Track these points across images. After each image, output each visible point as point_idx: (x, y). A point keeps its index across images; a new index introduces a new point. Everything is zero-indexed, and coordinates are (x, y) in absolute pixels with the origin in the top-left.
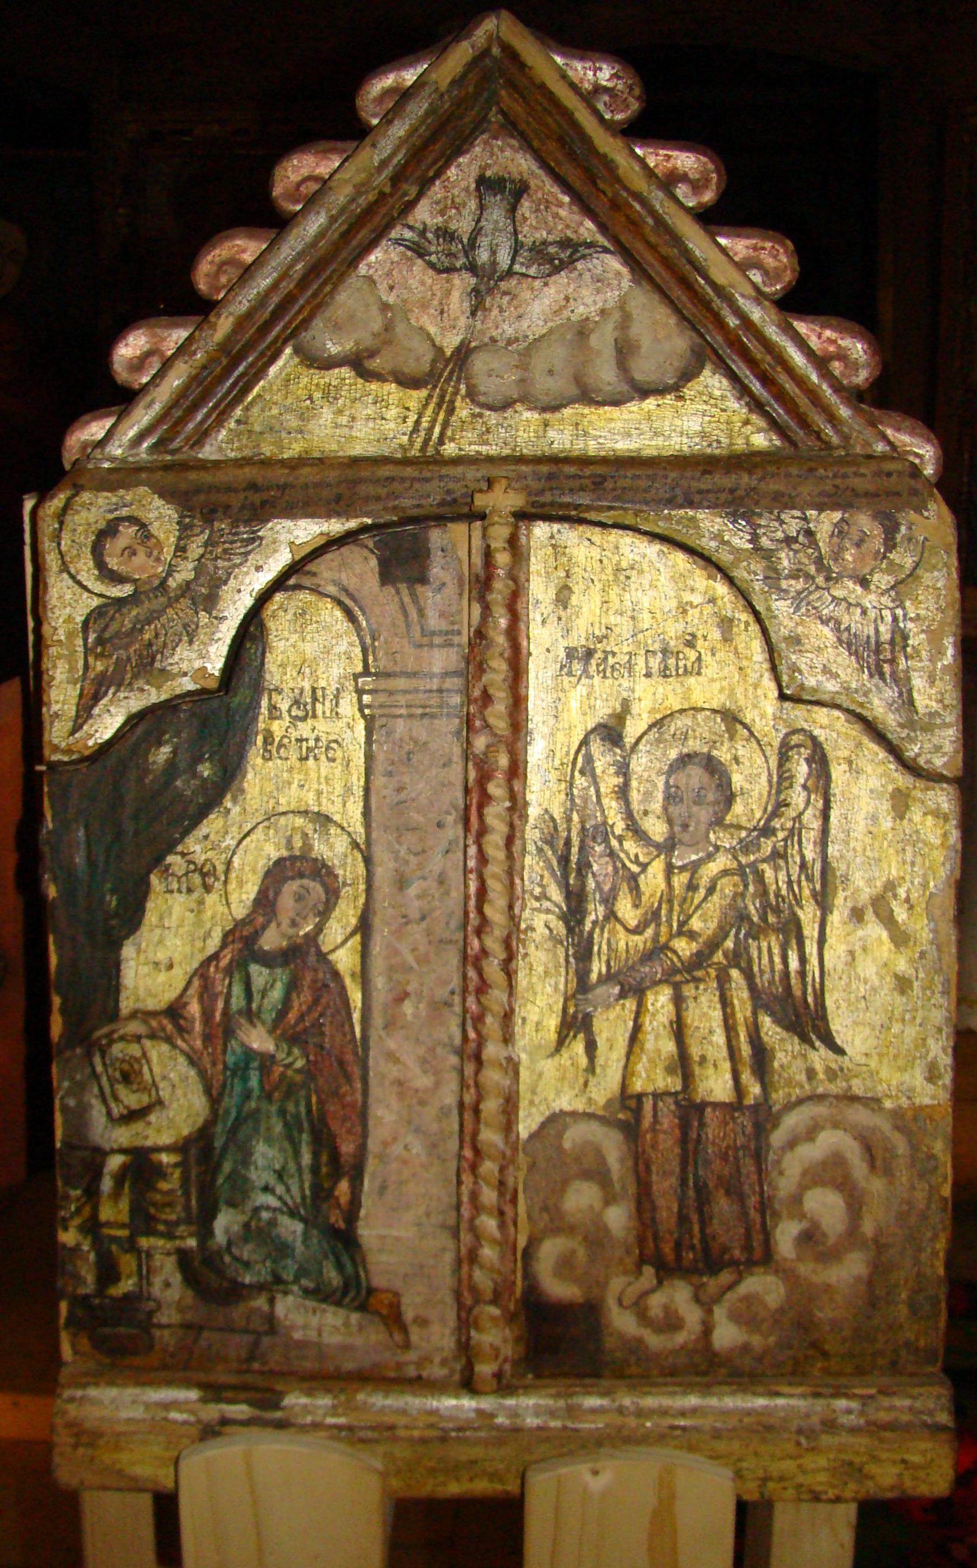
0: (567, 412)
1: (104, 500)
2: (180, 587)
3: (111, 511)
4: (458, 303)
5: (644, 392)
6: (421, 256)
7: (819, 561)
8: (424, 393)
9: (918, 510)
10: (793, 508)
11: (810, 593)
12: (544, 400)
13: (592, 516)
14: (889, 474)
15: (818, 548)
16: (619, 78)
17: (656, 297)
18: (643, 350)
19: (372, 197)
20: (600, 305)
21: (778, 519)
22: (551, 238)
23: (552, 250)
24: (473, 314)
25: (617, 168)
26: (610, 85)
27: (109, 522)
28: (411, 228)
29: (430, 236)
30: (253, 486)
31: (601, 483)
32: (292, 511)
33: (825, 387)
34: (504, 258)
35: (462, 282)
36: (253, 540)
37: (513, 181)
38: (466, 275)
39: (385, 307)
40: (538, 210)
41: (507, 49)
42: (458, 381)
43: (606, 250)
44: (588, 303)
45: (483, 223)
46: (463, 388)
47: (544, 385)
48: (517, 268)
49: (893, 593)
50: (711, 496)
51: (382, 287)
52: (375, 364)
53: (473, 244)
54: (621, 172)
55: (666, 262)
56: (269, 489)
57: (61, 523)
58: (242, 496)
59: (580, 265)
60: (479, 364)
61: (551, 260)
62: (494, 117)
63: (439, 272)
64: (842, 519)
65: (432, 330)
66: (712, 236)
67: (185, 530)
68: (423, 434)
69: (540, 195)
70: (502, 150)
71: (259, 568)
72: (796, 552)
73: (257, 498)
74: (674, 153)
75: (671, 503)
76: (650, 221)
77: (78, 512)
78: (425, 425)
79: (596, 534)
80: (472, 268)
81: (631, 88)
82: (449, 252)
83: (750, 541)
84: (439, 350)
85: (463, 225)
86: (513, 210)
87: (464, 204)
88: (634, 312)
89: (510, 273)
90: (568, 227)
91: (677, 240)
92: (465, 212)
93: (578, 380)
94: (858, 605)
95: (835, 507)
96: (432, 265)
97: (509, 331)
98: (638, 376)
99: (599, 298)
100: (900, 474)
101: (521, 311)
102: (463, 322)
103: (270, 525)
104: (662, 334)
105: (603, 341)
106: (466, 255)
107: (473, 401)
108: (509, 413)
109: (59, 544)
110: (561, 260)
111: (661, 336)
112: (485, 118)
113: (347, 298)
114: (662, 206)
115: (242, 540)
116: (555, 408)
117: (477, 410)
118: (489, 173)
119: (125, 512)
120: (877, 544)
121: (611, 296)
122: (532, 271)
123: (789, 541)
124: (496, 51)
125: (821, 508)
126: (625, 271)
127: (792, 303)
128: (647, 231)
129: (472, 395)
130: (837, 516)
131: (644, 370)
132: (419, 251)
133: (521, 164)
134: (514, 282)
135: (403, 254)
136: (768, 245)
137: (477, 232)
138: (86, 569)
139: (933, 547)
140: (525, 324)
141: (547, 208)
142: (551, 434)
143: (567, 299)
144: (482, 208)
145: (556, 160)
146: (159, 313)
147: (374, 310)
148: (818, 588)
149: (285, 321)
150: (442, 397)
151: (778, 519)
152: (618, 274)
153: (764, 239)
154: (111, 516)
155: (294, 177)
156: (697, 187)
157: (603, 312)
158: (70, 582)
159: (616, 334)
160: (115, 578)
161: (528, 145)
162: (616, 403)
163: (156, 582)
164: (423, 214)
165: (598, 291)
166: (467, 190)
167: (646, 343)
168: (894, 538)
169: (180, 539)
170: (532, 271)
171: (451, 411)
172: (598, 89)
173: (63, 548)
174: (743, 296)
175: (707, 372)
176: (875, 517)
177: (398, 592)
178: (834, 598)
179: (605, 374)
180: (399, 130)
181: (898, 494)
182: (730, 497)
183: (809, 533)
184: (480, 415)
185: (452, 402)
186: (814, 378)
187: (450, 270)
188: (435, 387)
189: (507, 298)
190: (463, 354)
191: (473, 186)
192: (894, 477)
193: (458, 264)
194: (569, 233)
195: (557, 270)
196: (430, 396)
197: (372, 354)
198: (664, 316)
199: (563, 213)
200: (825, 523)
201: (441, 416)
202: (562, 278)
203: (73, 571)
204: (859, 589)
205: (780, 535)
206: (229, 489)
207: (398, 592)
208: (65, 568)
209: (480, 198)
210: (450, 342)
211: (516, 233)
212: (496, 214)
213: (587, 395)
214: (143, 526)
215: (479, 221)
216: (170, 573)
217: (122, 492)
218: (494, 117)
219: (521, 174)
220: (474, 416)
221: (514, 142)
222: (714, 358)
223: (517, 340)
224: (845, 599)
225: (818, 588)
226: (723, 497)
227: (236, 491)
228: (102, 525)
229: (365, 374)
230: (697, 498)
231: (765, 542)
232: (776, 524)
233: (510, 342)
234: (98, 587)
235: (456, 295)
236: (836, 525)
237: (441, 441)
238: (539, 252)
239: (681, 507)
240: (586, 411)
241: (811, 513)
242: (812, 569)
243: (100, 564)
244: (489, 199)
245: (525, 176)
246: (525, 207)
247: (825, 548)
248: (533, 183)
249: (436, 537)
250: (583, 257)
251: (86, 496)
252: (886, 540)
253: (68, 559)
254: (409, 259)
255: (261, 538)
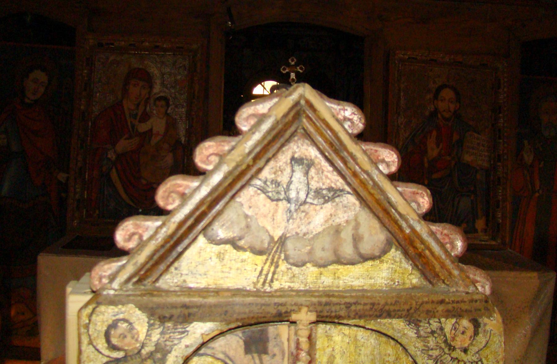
0: (331, 267)
1: (111, 310)
2: (147, 353)
3: (115, 316)
4: (281, 216)
5: (364, 258)
6: (264, 193)
7: (446, 341)
8: (264, 257)
9: (489, 318)
10: (435, 317)
11: (442, 356)
12: (322, 262)
13: (345, 322)
14: (476, 301)
15: (445, 336)
16: (355, 114)
17: (371, 215)
18: (365, 240)
19: (244, 167)
20: (346, 218)
21: (429, 323)
22: (324, 187)
23: (324, 192)
24: (288, 221)
25: (357, 159)
26: (351, 117)
27: (114, 321)
28: (260, 179)
29: (268, 183)
30: (185, 306)
31: (349, 307)
32: (202, 319)
33: (448, 261)
34: (302, 196)
35: (283, 205)
36: (183, 333)
37: (307, 160)
38: (285, 202)
39: (247, 216)
40: (318, 173)
41: (308, 102)
42: (281, 252)
43: (349, 193)
44: (342, 218)
45: (293, 179)
46: (283, 256)
47: (319, 254)
48: (308, 200)
49: (477, 355)
50: (400, 313)
51: (246, 206)
52: (242, 243)
53: (288, 189)
54: (359, 161)
55: (378, 202)
56: (192, 307)
57: (90, 320)
58: (179, 310)
59: (337, 200)
60: (290, 245)
61: (324, 197)
62: (300, 131)
63: (273, 200)
64: (456, 322)
65: (269, 228)
66: (395, 187)
67: (151, 326)
68: (263, 277)
69: (319, 166)
70: (302, 145)
71: (187, 346)
72: (436, 338)
73: (186, 312)
74: (379, 149)
75: (380, 316)
76: (371, 182)
77: (98, 315)
78: (264, 272)
79: (346, 330)
80: (289, 200)
81: (360, 119)
82: (278, 194)
83: (416, 333)
84: (272, 238)
85: (284, 179)
86: (307, 173)
87: (285, 170)
88: (361, 222)
89: (305, 202)
90: (332, 182)
91: (382, 192)
92: (285, 173)
93: (335, 252)
94: (463, 361)
95: (454, 316)
96: (269, 197)
97: (305, 230)
98: (363, 251)
99: (345, 215)
100: (481, 301)
101: (310, 220)
102: (284, 224)
103: (192, 325)
104: (373, 232)
105: (347, 235)
106: (285, 193)
107: (287, 262)
108: (304, 267)
109: (88, 331)
110: (329, 197)
111: (373, 234)
112: (296, 131)
113: (231, 214)
114: (377, 177)
115: (179, 332)
116: (324, 266)
117: (289, 266)
118: (296, 156)
119: (121, 316)
120: (470, 332)
121: (351, 214)
122: (315, 202)
123: (433, 332)
124: (303, 102)
125: (447, 317)
126: (357, 203)
127: (429, 217)
128: (370, 187)
129: (287, 258)
130: (454, 321)
131: (366, 248)
132: (263, 191)
133: (313, 152)
134: (307, 206)
135: (256, 192)
136: (420, 191)
137: (290, 183)
138: (102, 344)
139: (494, 334)
140: (311, 226)
141: (322, 172)
142: (323, 278)
143: (331, 215)
144: (293, 171)
145: (329, 153)
146: (138, 214)
147: (242, 218)
148: (445, 353)
149: (199, 220)
150: (273, 260)
151: (429, 323)
152: (355, 204)
153: (418, 189)
154: (114, 318)
155: (206, 153)
156: (388, 165)
157: (347, 222)
158: (93, 349)
159: (353, 232)
160: (114, 348)
161: (314, 143)
162: (353, 264)
163: (136, 351)
164: (266, 173)
165: (345, 212)
166: (286, 163)
167: (366, 236)
168: (478, 330)
169: (148, 331)
170: (315, 202)
171: (277, 266)
172: (345, 119)
173: (90, 333)
174: (412, 219)
175: (393, 250)
176: (470, 321)
177: (253, 358)
178: (452, 358)
179: (348, 250)
180: (257, 136)
181: (480, 310)
182: (407, 314)
183: (442, 329)
184: (291, 269)
185: (277, 262)
186: (443, 257)
187: (278, 200)
188: (269, 254)
189: (304, 214)
190: (283, 240)
191: (289, 161)
192: (478, 302)
193: (282, 197)
194: (333, 185)
195: (326, 202)
196: (267, 259)
197: (240, 239)
198: (375, 224)
199: (329, 175)
200: (448, 324)
201: (272, 269)
202: (329, 205)
203: (95, 344)
204: (463, 354)
205: (429, 330)
206: (174, 306)
207: (253, 358)
208: (91, 343)
209: (292, 166)
210: (277, 234)
211: (308, 184)
212: (299, 175)
213: (339, 261)
214: (130, 324)
215: (291, 178)
216: (142, 347)
217: (120, 306)
218: (300, 131)
219: (311, 156)
220: (288, 269)
221: (307, 141)
222: (397, 244)
223: (308, 233)
224: (457, 358)
225: (445, 353)
226: (404, 313)
227: (176, 307)
228: (110, 322)
229: (237, 248)
230: (393, 313)
231: (422, 333)
232: (427, 325)
233: (305, 234)
234: (107, 352)
235: (280, 211)
236: (453, 325)
237: (272, 281)
238: (318, 192)
239: (385, 318)
240: (340, 267)
241: (443, 320)
242: (443, 345)
243: (108, 341)
244: (296, 168)
245: (313, 158)
246: (312, 172)
247: (448, 335)
248: (316, 161)
249: (272, 329)
250: (339, 196)
251: (102, 308)
252: (475, 331)
253: (92, 338)
254: (259, 194)
255: (188, 331)
